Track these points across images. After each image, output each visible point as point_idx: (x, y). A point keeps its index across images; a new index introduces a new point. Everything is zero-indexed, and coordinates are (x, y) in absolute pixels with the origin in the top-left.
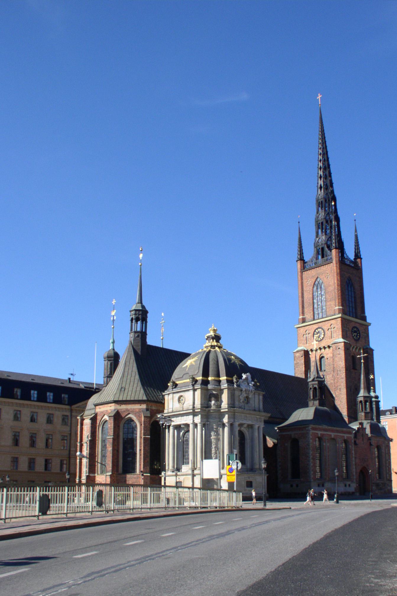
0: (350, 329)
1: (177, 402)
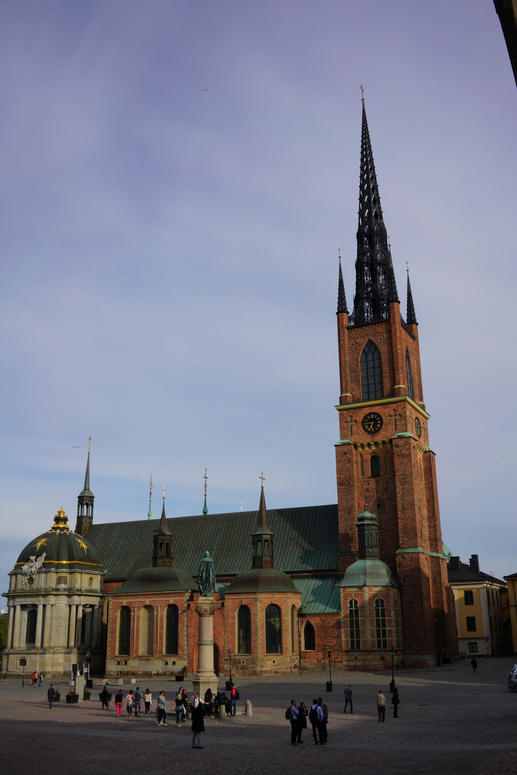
0: (360, 420)
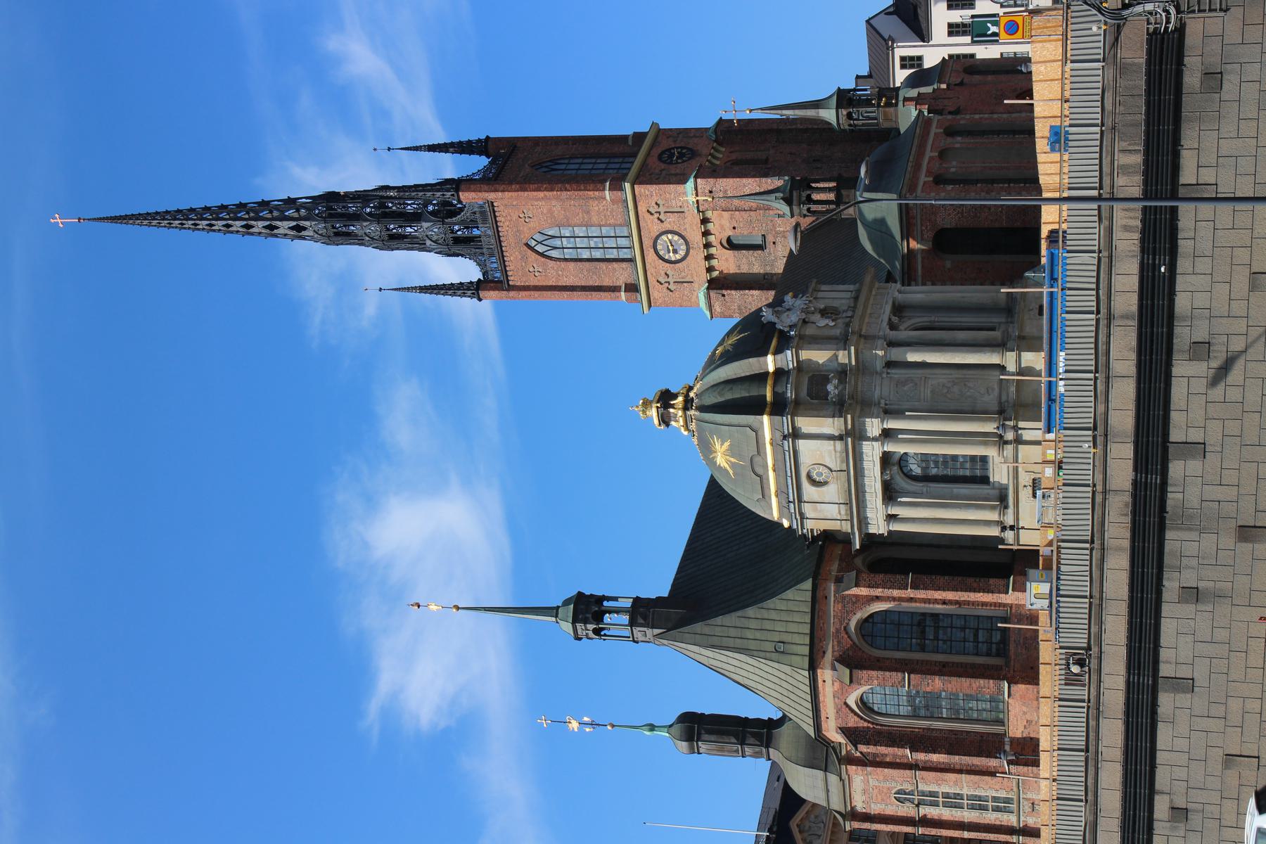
0: (663, 166)
1: (824, 489)
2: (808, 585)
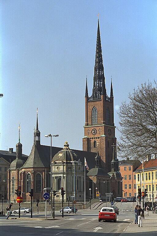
2: (44, 167)
